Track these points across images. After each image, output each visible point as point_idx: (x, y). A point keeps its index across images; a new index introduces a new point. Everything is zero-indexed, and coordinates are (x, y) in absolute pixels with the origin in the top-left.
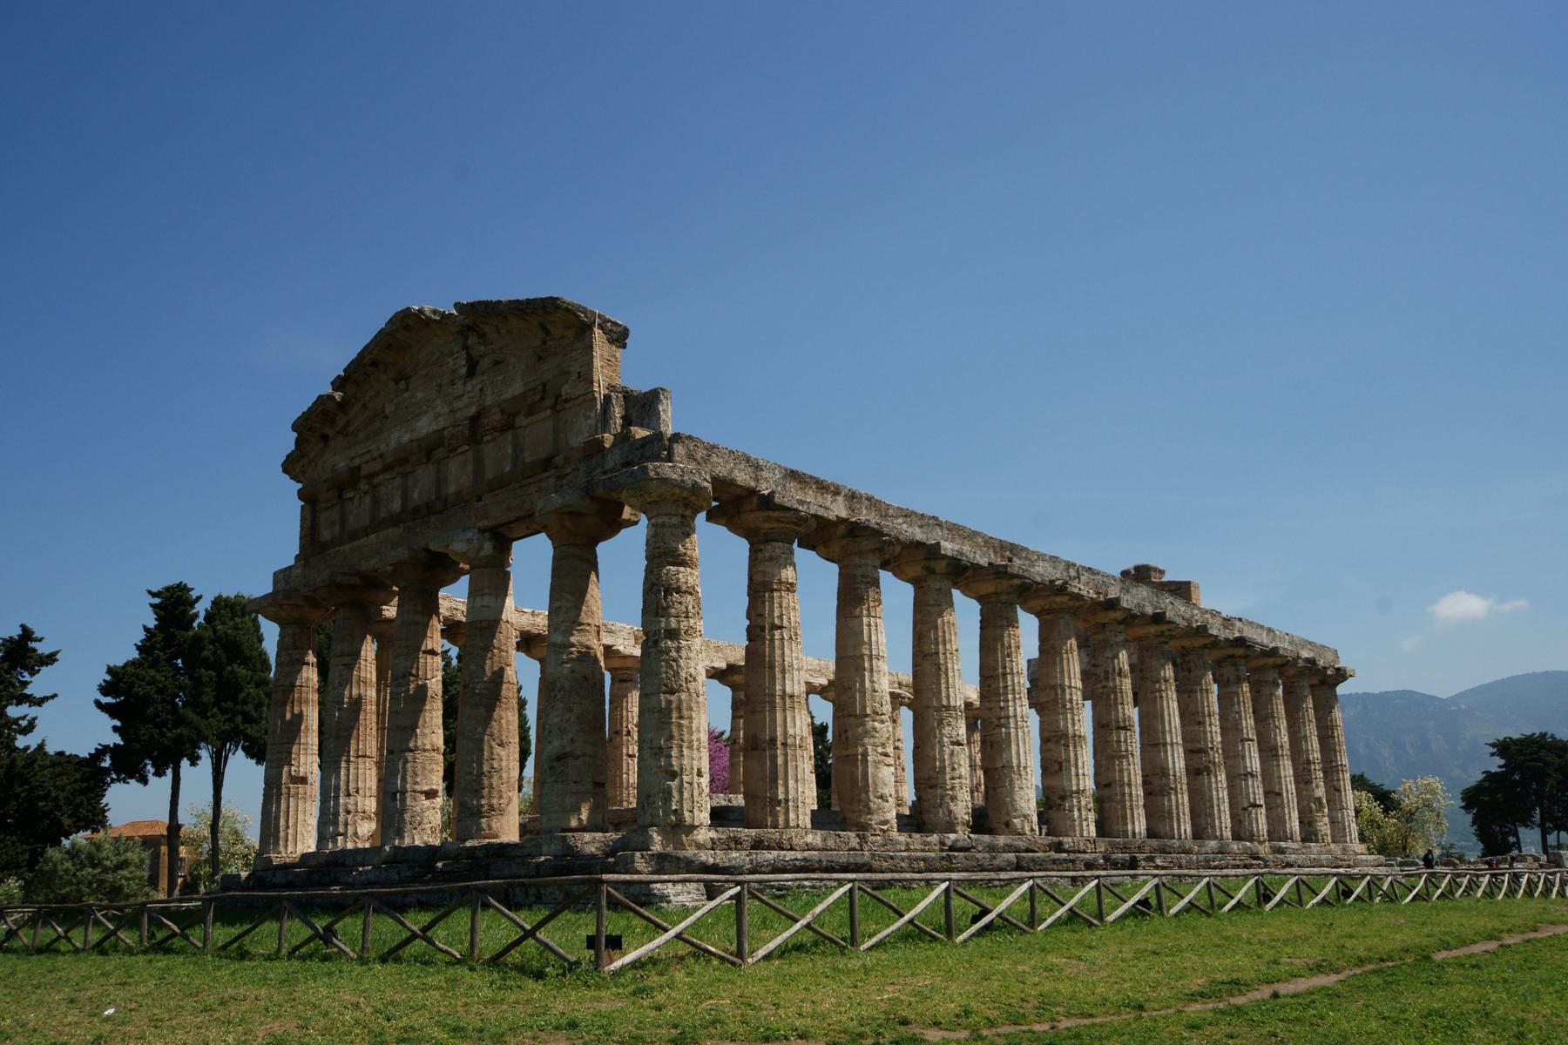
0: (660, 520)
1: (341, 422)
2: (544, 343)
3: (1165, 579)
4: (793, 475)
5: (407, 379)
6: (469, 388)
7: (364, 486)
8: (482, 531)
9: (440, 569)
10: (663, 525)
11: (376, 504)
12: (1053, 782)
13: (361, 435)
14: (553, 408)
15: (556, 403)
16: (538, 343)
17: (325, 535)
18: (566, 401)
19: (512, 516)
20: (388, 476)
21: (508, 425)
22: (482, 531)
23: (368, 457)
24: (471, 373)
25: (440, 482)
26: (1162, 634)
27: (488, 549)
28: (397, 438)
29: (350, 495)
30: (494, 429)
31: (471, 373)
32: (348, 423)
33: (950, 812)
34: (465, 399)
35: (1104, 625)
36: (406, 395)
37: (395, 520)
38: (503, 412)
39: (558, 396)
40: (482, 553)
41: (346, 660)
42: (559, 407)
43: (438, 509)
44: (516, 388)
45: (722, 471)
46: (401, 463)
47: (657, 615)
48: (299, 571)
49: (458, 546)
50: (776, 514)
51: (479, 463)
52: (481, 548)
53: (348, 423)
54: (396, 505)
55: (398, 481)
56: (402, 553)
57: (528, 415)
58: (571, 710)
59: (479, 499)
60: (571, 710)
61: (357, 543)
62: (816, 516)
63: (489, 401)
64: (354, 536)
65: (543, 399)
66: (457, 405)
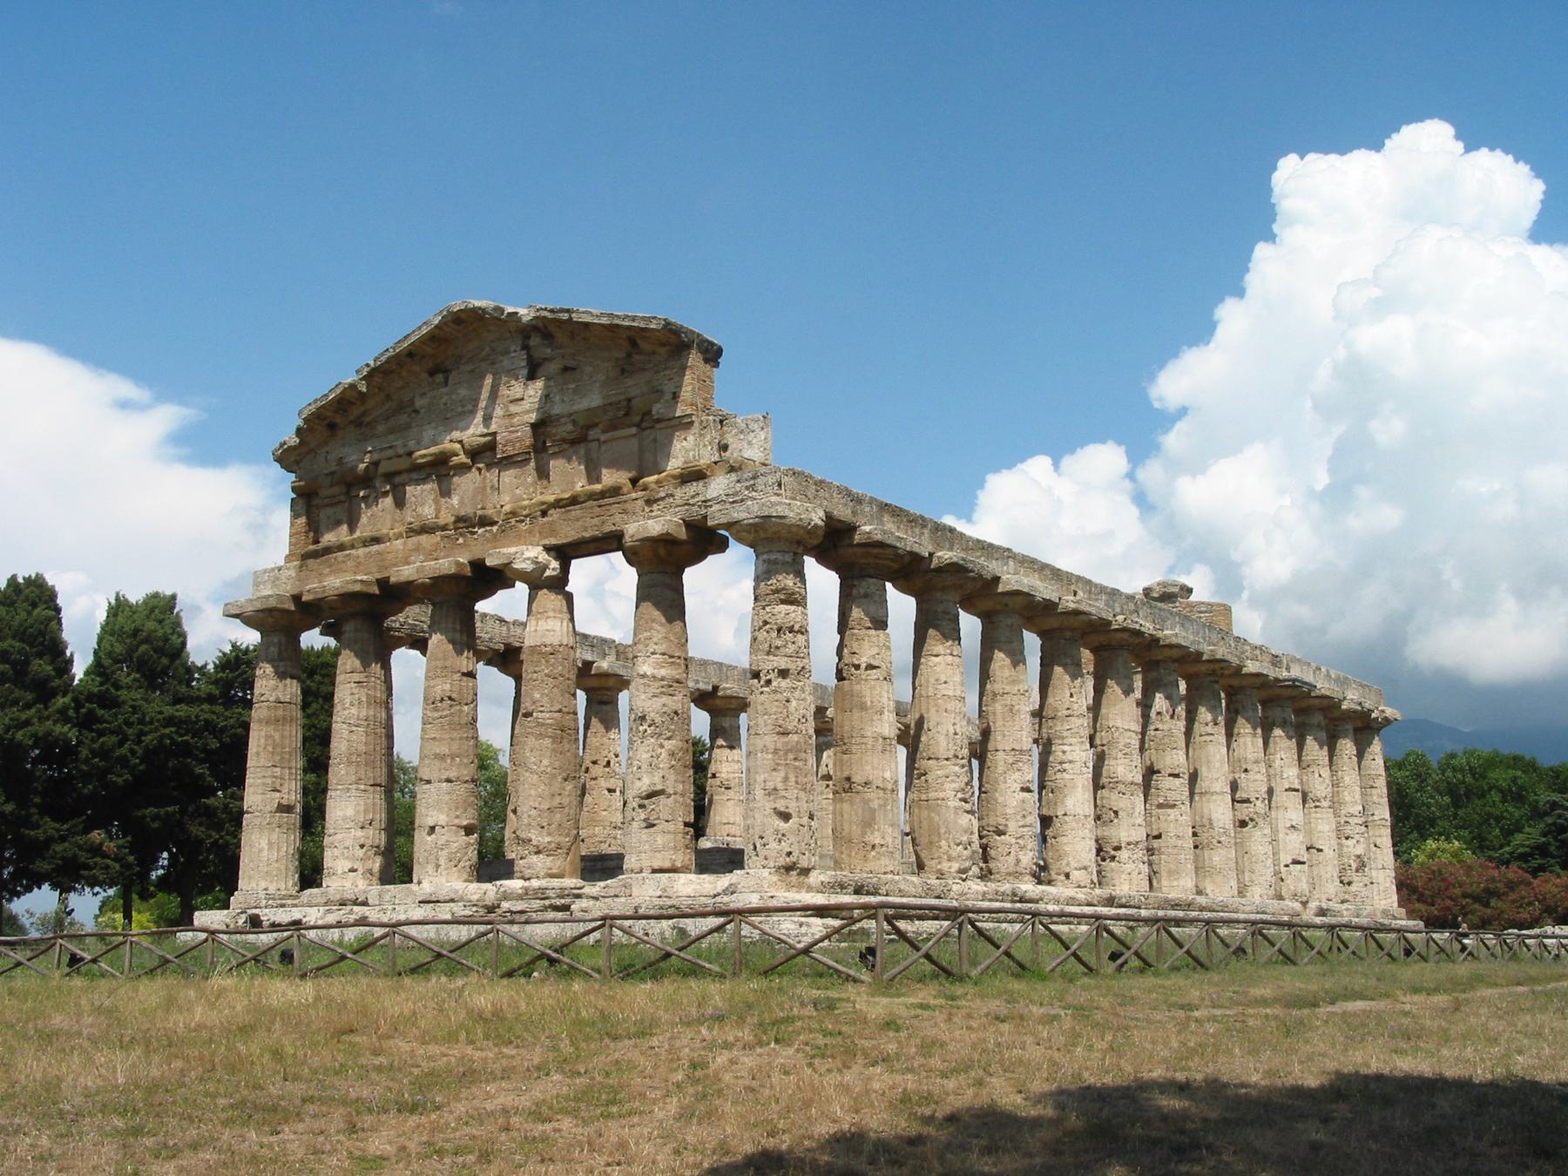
0: (773, 557)
1: (356, 411)
2: (629, 355)
4: (885, 508)
5: (446, 372)
8: (548, 549)
10: (775, 562)
12: (1106, 832)
13: (381, 428)
14: (638, 425)
15: (642, 421)
16: (621, 355)
18: (658, 421)
19: (587, 535)
20: (415, 476)
23: (390, 453)
26: (1214, 673)
30: (564, 440)
32: (364, 414)
33: (1018, 861)
34: (526, 405)
35: (1158, 662)
36: (445, 390)
38: (574, 422)
39: (649, 412)
40: (548, 573)
42: (644, 425)
44: (594, 400)
47: (768, 653)
48: (293, 573)
50: (875, 551)
52: (546, 567)
53: (364, 414)
56: (445, 565)
57: (605, 431)
58: (662, 746)
59: (544, 513)
60: (662, 746)
61: (375, 548)
62: (911, 553)
63: (557, 409)
64: (376, 540)
65: (627, 414)
66: (514, 408)
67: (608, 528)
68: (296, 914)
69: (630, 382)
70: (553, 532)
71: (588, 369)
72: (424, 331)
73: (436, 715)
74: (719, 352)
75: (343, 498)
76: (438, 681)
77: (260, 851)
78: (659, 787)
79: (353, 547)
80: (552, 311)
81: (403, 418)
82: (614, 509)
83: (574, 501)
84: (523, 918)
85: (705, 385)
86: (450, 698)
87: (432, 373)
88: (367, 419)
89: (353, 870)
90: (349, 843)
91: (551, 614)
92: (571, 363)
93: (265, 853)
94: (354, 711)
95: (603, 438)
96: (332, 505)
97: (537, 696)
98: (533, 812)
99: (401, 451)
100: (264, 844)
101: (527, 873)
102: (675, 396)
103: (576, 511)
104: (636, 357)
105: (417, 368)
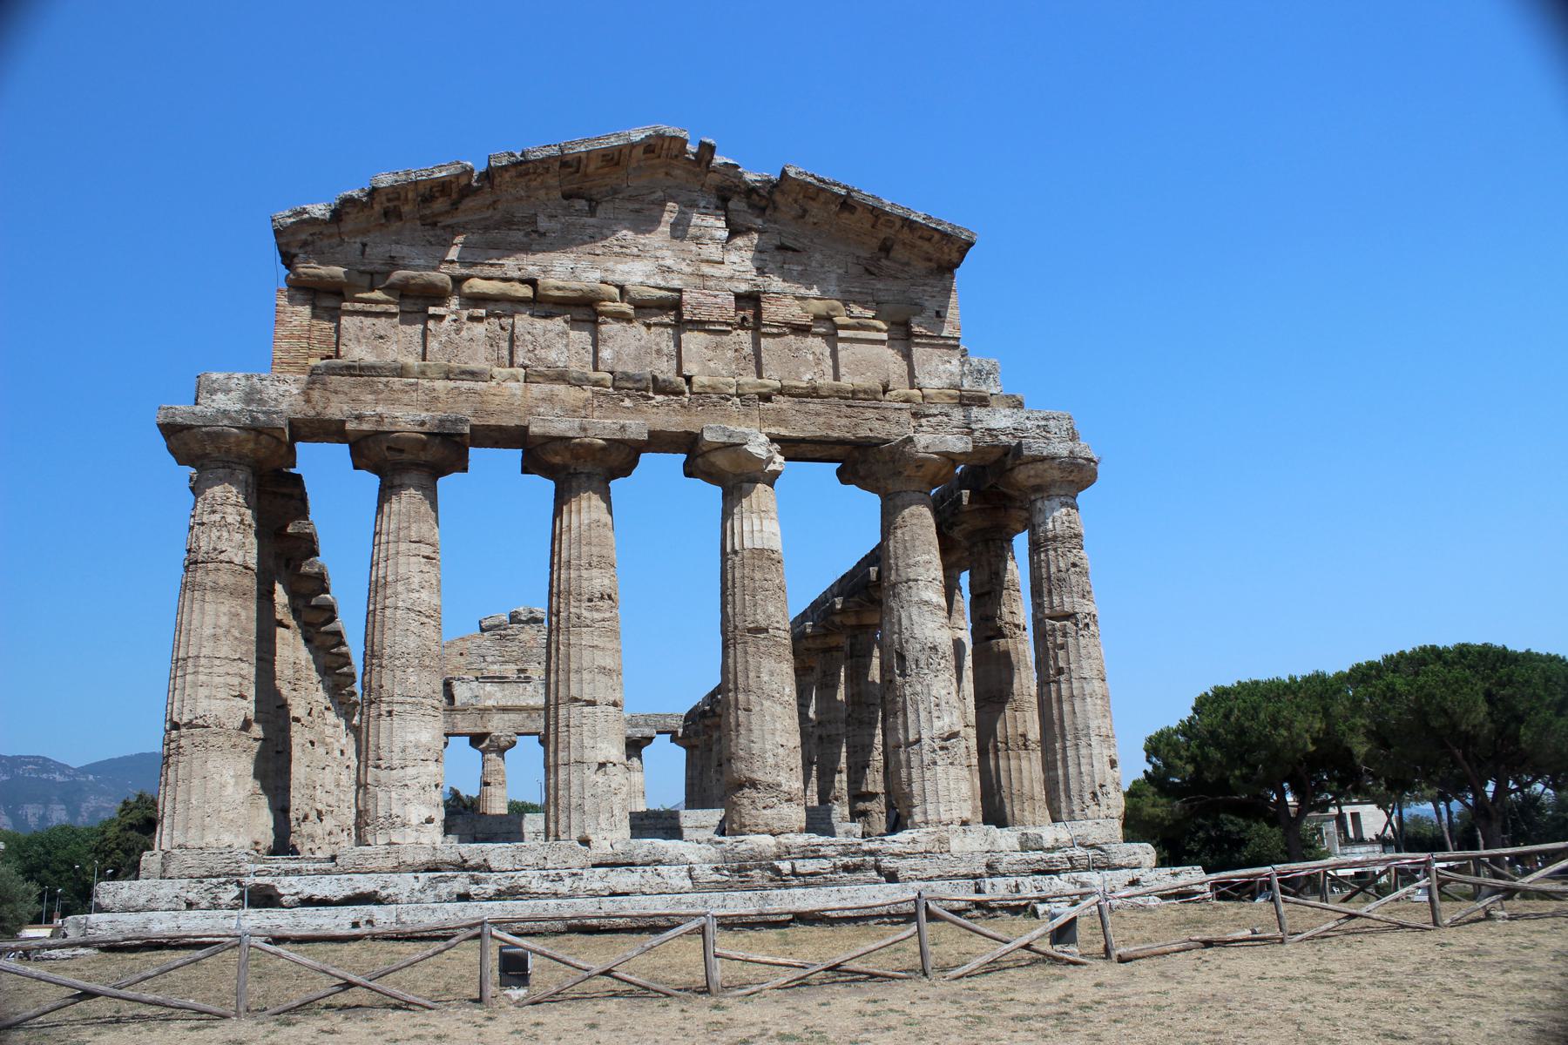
1: (440, 205)
6: (733, 257)
7: (454, 303)
8: (774, 439)
16: (864, 254)
17: (358, 352)
19: (835, 434)
22: (774, 439)
28: (563, 270)
29: (440, 311)
30: (787, 324)
32: (447, 212)
36: (591, 221)
39: (906, 325)
41: (427, 550)
47: (1084, 597)
55: (558, 324)
59: (766, 398)
61: (466, 385)
66: (706, 269)
67: (863, 432)
68: (365, 884)
69: (880, 286)
70: (781, 422)
71: (818, 256)
72: (614, 142)
73: (597, 616)
75: (394, 309)
76: (595, 572)
77: (223, 786)
78: (956, 729)
79: (423, 374)
80: (824, 181)
81: (517, 236)
82: (869, 414)
83: (813, 393)
84: (819, 879)
86: (610, 597)
87: (567, 196)
88: (449, 221)
89: (429, 821)
90: (424, 780)
91: (773, 515)
92: (789, 243)
93: (230, 790)
94: (424, 595)
95: (842, 333)
96: (367, 314)
97: (771, 609)
98: (781, 750)
99: (516, 274)
100: (228, 776)
101: (776, 826)
102: (940, 315)
103: (815, 405)
104: (884, 262)
105: (553, 182)
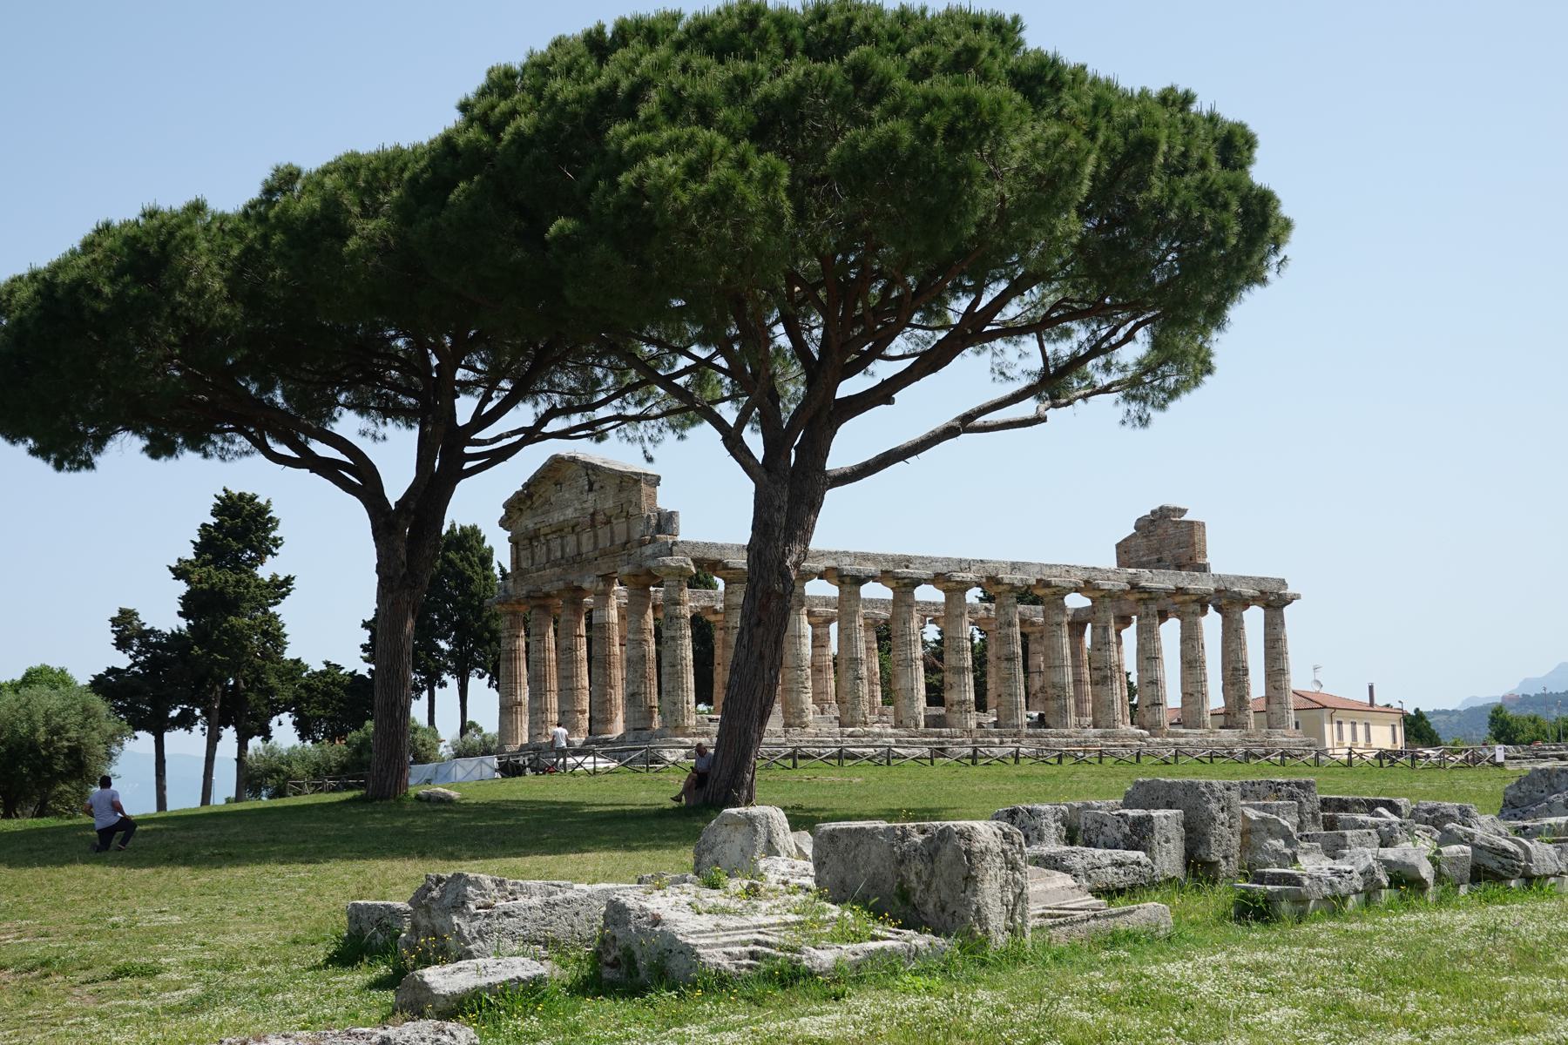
3: (1186, 518)
9: (579, 591)
11: (549, 550)
21: (608, 522)
24: (591, 490)
25: (579, 544)
27: (601, 586)
28: (557, 517)
31: (591, 490)
37: (555, 564)
43: (578, 561)
45: (698, 555)
46: (559, 530)
49: (586, 585)
51: (596, 536)
54: (559, 554)
74: (659, 478)
85: (653, 497)
